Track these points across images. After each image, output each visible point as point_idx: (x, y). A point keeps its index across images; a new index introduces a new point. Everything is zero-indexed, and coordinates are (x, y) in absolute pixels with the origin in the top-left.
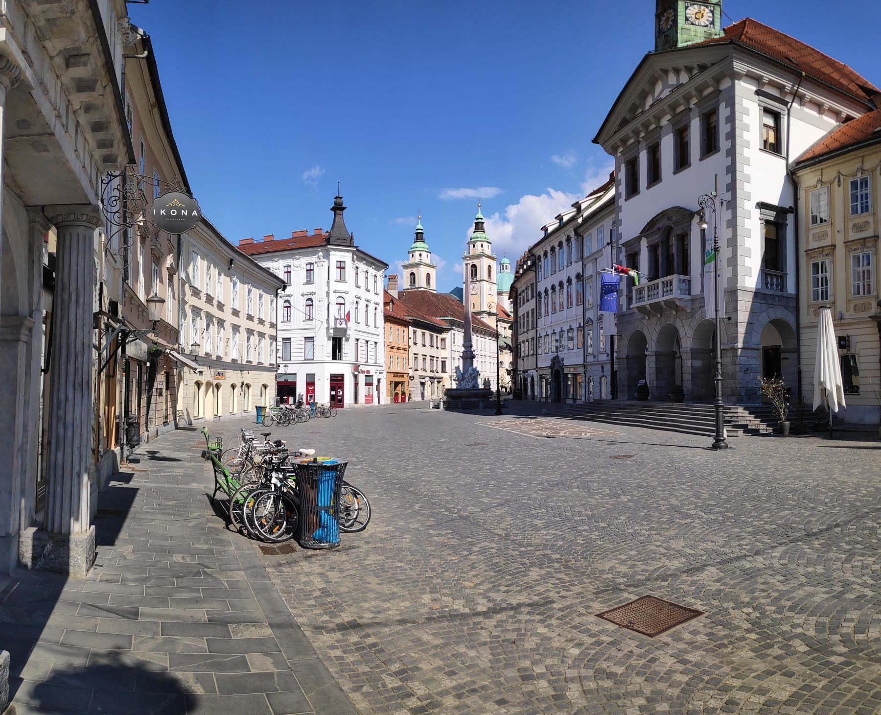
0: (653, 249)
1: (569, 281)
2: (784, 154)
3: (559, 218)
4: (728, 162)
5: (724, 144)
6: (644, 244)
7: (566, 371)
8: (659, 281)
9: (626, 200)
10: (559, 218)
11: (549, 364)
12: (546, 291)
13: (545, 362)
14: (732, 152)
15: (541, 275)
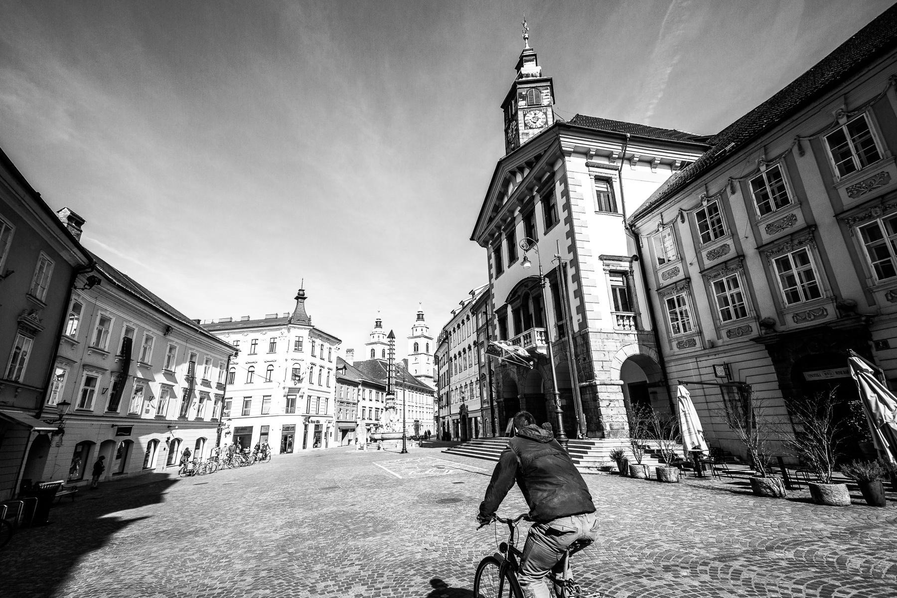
0: (516, 312)
1: (470, 348)
2: (620, 211)
3: (462, 303)
4: (568, 228)
5: (562, 215)
6: (509, 309)
7: (470, 415)
8: (521, 336)
9: (496, 278)
10: (462, 303)
11: (458, 411)
12: (455, 357)
13: (455, 409)
14: (569, 220)
15: (452, 345)
